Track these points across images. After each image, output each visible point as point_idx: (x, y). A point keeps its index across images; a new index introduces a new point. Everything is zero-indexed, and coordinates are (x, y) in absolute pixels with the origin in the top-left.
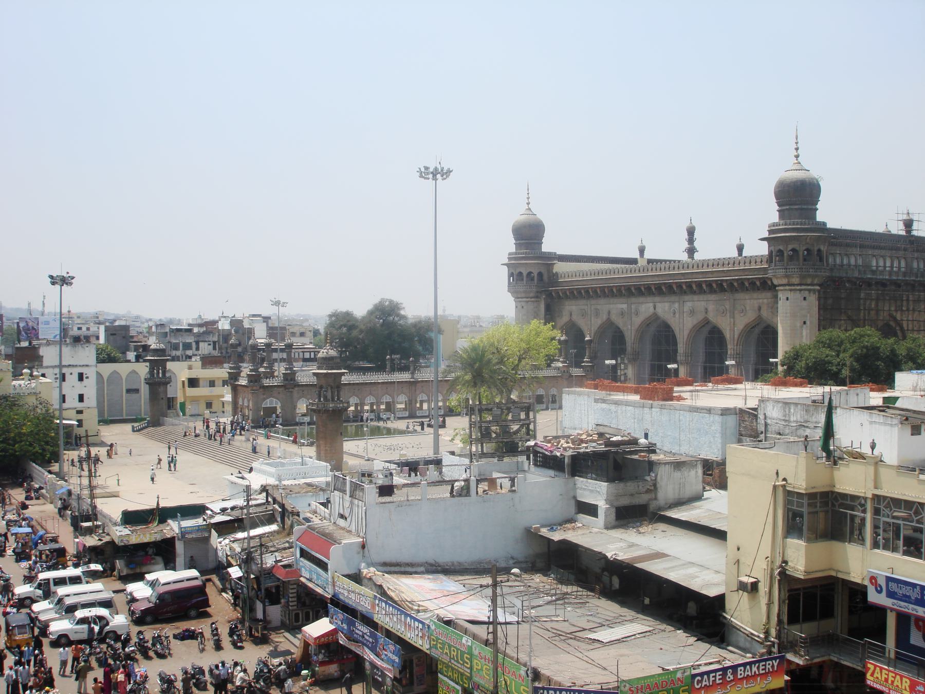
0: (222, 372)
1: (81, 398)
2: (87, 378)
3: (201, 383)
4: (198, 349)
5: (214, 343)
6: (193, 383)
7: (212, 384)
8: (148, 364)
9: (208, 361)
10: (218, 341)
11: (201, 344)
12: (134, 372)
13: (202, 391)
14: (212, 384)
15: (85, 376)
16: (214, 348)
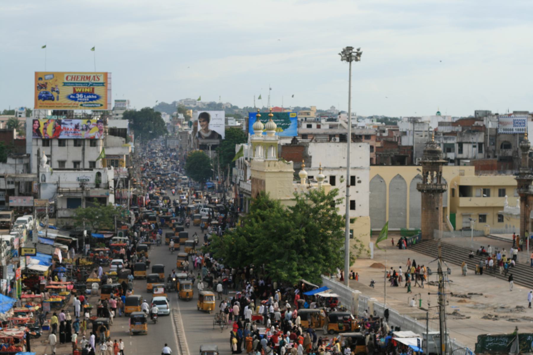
0: (509, 179)
1: (353, 205)
2: (359, 182)
3: (474, 192)
4: (461, 151)
5: (480, 145)
6: (465, 191)
7: (486, 191)
8: (421, 168)
9: (481, 168)
10: (485, 143)
11: (465, 146)
12: (399, 177)
13: (476, 201)
14: (486, 191)
15: (357, 180)
16: (480, 151)
